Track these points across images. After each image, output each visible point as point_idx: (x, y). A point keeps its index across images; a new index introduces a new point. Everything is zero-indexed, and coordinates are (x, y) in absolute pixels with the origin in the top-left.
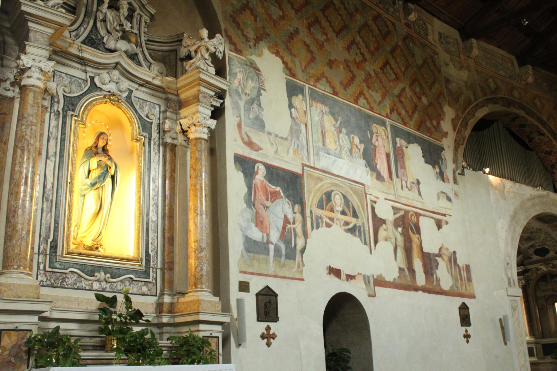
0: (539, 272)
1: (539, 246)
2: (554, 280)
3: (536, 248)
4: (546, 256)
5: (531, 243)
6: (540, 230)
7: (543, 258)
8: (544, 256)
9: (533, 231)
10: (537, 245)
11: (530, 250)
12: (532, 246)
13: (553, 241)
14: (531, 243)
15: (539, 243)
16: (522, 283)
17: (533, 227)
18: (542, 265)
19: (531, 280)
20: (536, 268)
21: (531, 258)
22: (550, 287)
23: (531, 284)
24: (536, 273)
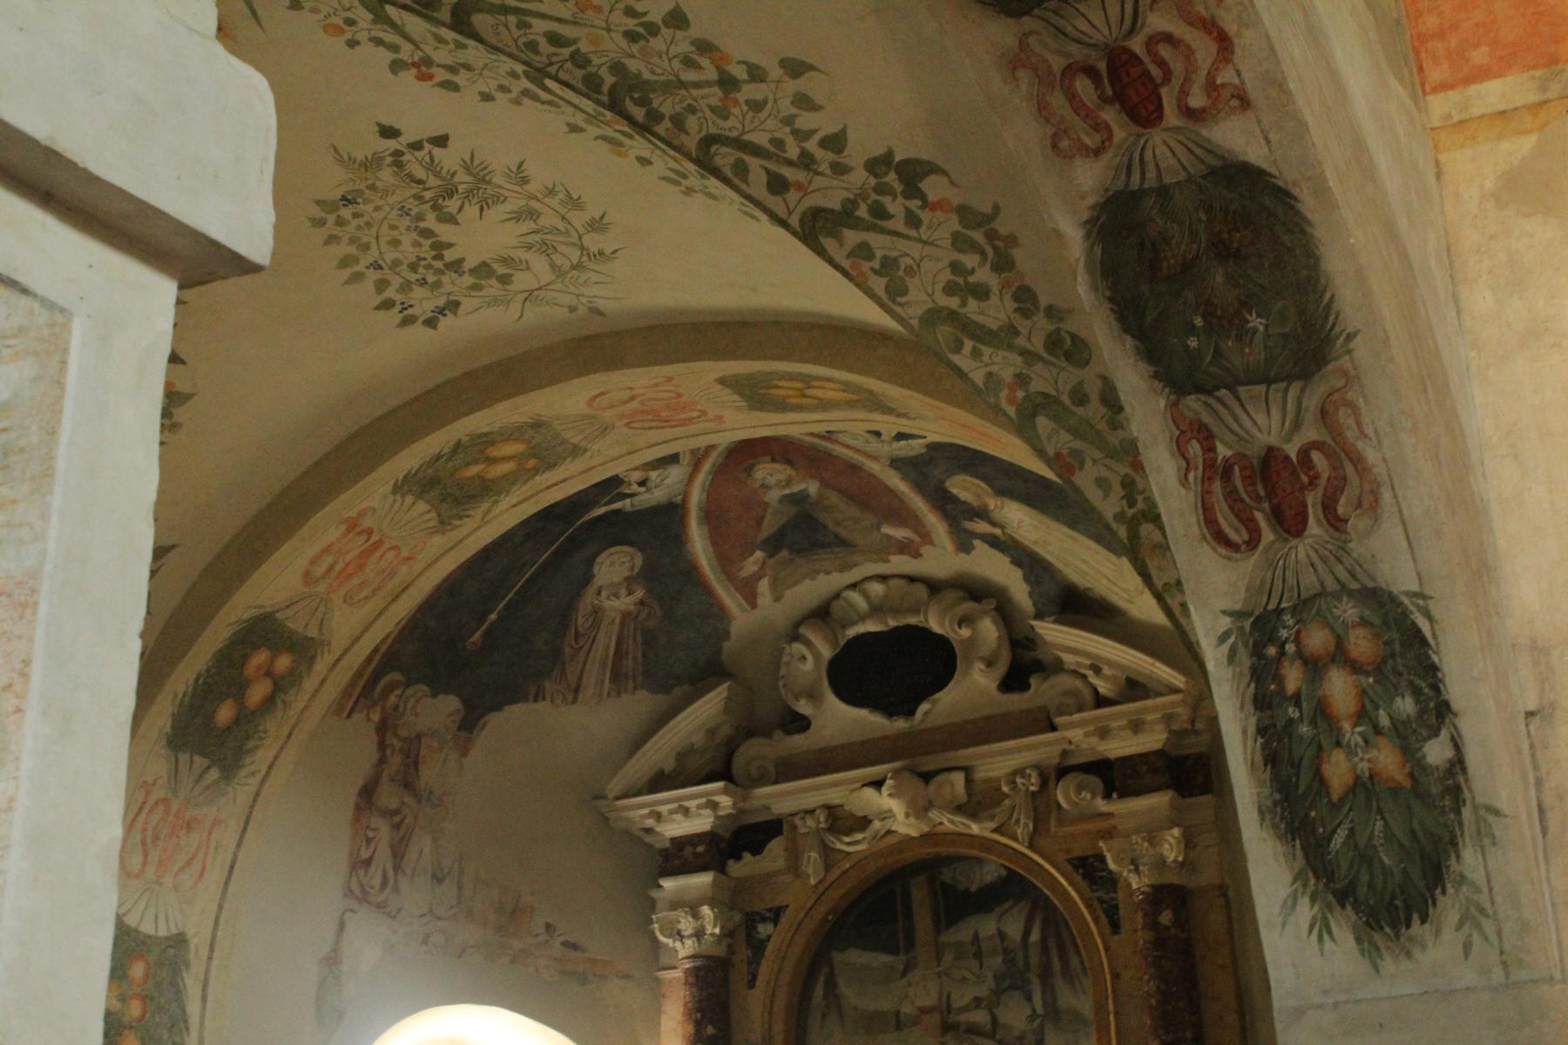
0: (854, 845)
1: (877, 610)
2: (962, 933)
3: (852, 632)
4: (924, 707)
5: (811, 590)
6: (912, 174)
7: (901, 724)
8: (910, 713)
9: (834, 202)
10: (855, 597)
11: (798, 647)
12: (822, 614)
13: (1035, 333)
14: (811, 590)
15: (877, 589)
16: (699, 934)
17: (835, 142)
18: (878, 784)
19: (776, 914)
20: (830, 809)
21: (800, 724)
22: (922, 992)
23: (770, 948)
24: (826, 851)
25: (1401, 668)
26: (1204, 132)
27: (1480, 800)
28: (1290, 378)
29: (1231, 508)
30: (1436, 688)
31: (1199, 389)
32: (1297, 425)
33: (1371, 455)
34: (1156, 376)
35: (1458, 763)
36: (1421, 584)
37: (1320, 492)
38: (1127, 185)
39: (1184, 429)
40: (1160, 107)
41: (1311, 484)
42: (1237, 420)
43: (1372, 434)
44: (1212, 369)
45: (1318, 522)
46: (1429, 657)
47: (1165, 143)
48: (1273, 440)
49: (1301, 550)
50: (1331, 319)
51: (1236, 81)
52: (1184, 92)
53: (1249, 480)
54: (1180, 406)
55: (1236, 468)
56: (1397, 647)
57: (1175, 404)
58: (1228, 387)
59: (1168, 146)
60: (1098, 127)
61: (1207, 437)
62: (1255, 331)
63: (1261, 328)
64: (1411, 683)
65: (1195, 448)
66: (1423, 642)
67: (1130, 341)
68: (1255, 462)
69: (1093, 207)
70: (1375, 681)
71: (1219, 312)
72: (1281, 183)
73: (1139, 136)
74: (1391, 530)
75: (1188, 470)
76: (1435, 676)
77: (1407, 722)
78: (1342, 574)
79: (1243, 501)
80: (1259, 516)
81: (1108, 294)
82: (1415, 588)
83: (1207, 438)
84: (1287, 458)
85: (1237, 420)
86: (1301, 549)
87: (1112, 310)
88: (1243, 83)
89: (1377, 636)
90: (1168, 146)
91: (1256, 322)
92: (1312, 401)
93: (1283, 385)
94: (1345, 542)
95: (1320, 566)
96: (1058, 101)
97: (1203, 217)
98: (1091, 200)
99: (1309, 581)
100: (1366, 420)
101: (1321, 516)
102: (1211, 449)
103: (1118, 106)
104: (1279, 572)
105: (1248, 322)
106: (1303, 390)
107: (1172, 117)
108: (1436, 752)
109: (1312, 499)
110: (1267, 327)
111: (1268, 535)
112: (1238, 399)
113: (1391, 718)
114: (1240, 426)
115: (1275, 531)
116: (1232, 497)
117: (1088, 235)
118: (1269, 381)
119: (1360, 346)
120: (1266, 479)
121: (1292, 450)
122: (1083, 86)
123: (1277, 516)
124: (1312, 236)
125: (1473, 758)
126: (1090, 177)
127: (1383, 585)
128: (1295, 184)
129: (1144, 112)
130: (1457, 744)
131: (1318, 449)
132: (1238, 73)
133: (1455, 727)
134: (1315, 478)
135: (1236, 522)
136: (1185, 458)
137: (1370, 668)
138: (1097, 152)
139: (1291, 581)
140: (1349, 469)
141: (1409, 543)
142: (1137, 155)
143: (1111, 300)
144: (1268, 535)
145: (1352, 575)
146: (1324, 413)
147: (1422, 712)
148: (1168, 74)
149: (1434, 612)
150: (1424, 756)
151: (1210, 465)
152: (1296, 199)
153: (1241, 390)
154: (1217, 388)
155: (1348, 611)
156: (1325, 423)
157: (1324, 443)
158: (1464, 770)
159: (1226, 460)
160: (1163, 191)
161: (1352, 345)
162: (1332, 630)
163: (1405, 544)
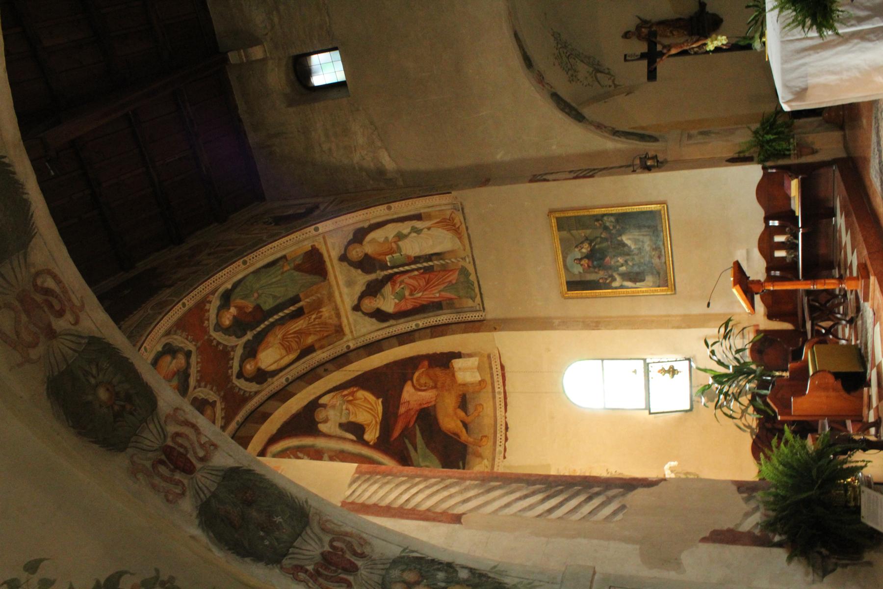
25: (427, 570)
26: (211, 464)
27: (488, 569)
28: (304, 528)
29: (332, 582)
30: (440, 563)
31: (285, 556)
32: (320, 540)
33: (348, 529)
34: (267, 564)
35: (472, 570)
36: (402, 547)
37: (348, 552)
38: (201, 500)
39: (292, 572)
40: (191, 463)
41: (343, 553)
42: (304, 555)
43: (342, 524)
44: (282, 545)
45: (358, 560)
46: (428, 560)
47: (203, 476)
48: (320, 551)
49: (363, 572)
50: (296, 500)
51: (207, 440)
52: (195, 453)
53: (326, 569)
54: (284, 566)
55: (320, 569)
56: (419, 567)
57: (281, 568)
58: (290, 548)
59: (204, 477)
60: (178, 483)
61: (301, 568)
62: (280, 523)
63: (281, 520)
64: (434, 570)
65: (302, 575)
66: (421, 558)
67: (248, 560)
68: (322, 562)
69: (197, 517)
70: (427, 579)
71: (265, 526)
72: (245, 468)
73: (192, 478)
74: (376, 543)
75: (307, 584)
76: (436, 561)
77: (448, 578)
78: (382, 566)
79: (332, 576)
80: (342, 576)
81: (226, 548)
82: (402, 549)
83: (301, 569)
84: (329, 552)
85: (304, 555)
86: (363, 572)
87: (233, 553)
88: (210, 439)
89: (410, 570)
90: (204, 477)
91: (278, 519)
92: (317, 530)
93: (304, 533)
94: (370, 557)
95: (373, 571)
96: (157, 481)
97: (233, 496)
98: (195, 514)
99: (376, 578)
100: (336, 521)
101: (356, 558)
102: (306, 571)
103: (178, 471)
104: (366, 585)
105: (276, 521)
106: (311, 529)
107: (199, 465)
108: (463, 574)
109: (348, 556)
110: (282, 518)
111: (351, 578)
112: (297, 548)
113: (442, 582)
114: (307, 555)
115: (351, 575)
116: (327, 578)
117: (203, 530)
118: (299, 535)
119: (310, 502)
120: (330, 563)
121: (327, 548)
122: (162, 469)
123: (346, 570)
124: (268, 479)
125: (471, 565)
126: (187, 505)
127: (393, 558)
128: (249, 465)
129: (189, 469)
130: (463, 567)
131: (335, 541)
132: (206, 436)
133: (457, 565)
134: (342, 550)
135: (338, 584)
136: (302, 581)
137: (420, 579)
138: (183, 494)
139: (372, 583)
140: (348, 539)
141: (386, 541)
142: (197, 487)
143: (229, 549)
144: (351, 578)
145: (384, 564)
146: (323, 530)
147: (446, 571)
148: (185, 448)
149: (413, 549)
150: (463, 579)
151: (311, 576)
152: (254, 470)
153: (295, 544)
154: (288, 550)
155: (395, 573)
156: (328, 532)
157: (333, 538)
158: (474, 569)
159: (314, 569)
160: (214, 495)
161: (309, 504)
162: (399, 582)
163: (385, 543)
